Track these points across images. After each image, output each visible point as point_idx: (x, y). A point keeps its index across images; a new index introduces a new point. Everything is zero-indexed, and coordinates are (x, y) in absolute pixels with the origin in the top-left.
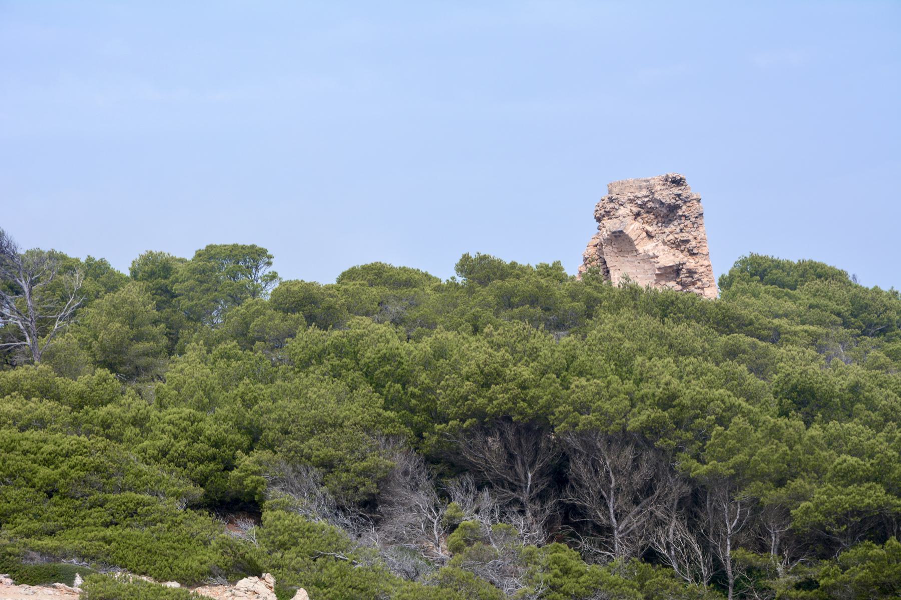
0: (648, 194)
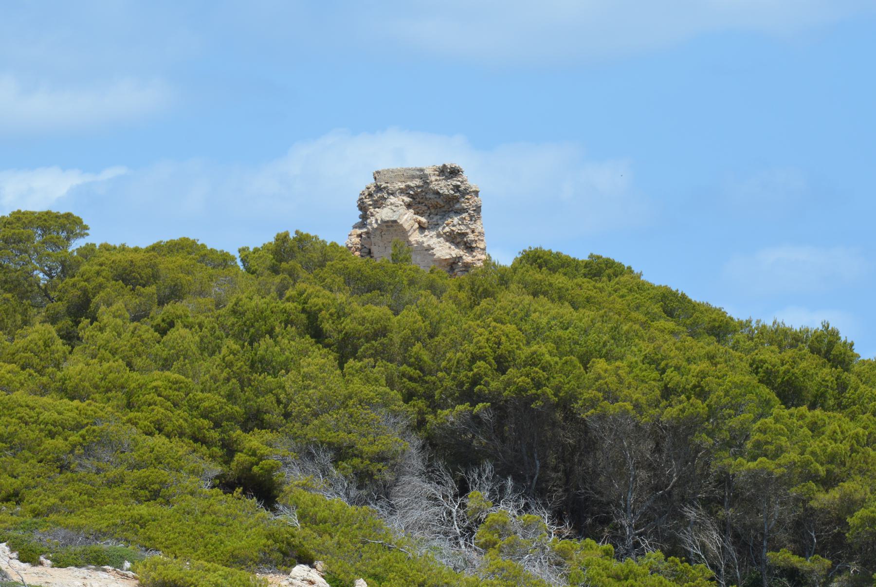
0: (421, 184)
